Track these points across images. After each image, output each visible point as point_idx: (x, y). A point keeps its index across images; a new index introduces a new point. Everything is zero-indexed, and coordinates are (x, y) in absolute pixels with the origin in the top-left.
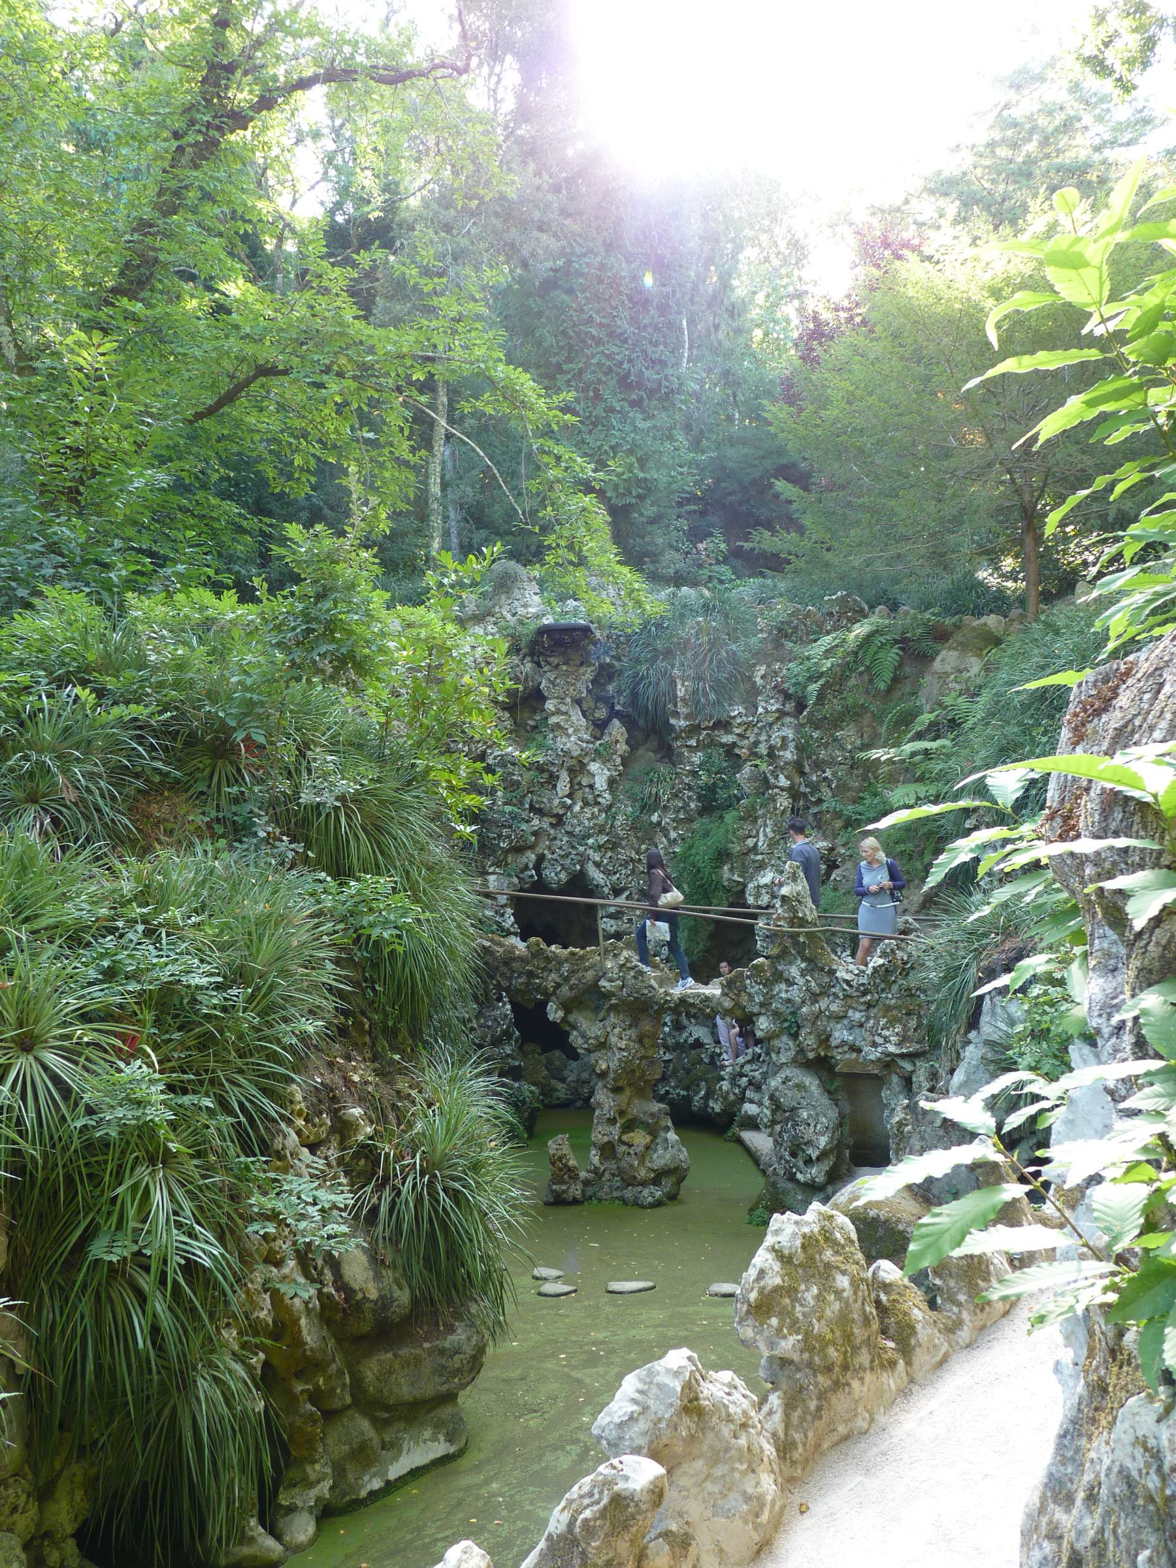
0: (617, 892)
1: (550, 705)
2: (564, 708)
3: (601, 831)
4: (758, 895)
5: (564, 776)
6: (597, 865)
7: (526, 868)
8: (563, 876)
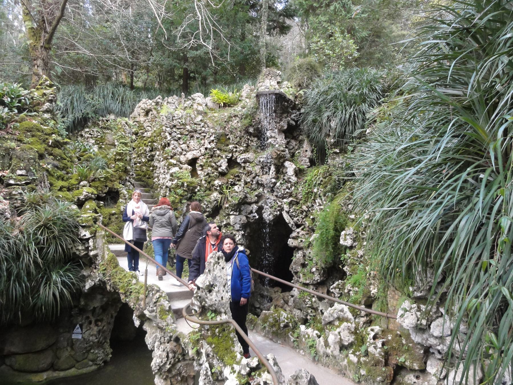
0: (298, 226)
1: (268, 134)
2: (273, 135)
3: (291, 195)
4: (345, 240)
5: (273, 168)
6: (288, 212)
7: (251, 212)
8: (271, 217)
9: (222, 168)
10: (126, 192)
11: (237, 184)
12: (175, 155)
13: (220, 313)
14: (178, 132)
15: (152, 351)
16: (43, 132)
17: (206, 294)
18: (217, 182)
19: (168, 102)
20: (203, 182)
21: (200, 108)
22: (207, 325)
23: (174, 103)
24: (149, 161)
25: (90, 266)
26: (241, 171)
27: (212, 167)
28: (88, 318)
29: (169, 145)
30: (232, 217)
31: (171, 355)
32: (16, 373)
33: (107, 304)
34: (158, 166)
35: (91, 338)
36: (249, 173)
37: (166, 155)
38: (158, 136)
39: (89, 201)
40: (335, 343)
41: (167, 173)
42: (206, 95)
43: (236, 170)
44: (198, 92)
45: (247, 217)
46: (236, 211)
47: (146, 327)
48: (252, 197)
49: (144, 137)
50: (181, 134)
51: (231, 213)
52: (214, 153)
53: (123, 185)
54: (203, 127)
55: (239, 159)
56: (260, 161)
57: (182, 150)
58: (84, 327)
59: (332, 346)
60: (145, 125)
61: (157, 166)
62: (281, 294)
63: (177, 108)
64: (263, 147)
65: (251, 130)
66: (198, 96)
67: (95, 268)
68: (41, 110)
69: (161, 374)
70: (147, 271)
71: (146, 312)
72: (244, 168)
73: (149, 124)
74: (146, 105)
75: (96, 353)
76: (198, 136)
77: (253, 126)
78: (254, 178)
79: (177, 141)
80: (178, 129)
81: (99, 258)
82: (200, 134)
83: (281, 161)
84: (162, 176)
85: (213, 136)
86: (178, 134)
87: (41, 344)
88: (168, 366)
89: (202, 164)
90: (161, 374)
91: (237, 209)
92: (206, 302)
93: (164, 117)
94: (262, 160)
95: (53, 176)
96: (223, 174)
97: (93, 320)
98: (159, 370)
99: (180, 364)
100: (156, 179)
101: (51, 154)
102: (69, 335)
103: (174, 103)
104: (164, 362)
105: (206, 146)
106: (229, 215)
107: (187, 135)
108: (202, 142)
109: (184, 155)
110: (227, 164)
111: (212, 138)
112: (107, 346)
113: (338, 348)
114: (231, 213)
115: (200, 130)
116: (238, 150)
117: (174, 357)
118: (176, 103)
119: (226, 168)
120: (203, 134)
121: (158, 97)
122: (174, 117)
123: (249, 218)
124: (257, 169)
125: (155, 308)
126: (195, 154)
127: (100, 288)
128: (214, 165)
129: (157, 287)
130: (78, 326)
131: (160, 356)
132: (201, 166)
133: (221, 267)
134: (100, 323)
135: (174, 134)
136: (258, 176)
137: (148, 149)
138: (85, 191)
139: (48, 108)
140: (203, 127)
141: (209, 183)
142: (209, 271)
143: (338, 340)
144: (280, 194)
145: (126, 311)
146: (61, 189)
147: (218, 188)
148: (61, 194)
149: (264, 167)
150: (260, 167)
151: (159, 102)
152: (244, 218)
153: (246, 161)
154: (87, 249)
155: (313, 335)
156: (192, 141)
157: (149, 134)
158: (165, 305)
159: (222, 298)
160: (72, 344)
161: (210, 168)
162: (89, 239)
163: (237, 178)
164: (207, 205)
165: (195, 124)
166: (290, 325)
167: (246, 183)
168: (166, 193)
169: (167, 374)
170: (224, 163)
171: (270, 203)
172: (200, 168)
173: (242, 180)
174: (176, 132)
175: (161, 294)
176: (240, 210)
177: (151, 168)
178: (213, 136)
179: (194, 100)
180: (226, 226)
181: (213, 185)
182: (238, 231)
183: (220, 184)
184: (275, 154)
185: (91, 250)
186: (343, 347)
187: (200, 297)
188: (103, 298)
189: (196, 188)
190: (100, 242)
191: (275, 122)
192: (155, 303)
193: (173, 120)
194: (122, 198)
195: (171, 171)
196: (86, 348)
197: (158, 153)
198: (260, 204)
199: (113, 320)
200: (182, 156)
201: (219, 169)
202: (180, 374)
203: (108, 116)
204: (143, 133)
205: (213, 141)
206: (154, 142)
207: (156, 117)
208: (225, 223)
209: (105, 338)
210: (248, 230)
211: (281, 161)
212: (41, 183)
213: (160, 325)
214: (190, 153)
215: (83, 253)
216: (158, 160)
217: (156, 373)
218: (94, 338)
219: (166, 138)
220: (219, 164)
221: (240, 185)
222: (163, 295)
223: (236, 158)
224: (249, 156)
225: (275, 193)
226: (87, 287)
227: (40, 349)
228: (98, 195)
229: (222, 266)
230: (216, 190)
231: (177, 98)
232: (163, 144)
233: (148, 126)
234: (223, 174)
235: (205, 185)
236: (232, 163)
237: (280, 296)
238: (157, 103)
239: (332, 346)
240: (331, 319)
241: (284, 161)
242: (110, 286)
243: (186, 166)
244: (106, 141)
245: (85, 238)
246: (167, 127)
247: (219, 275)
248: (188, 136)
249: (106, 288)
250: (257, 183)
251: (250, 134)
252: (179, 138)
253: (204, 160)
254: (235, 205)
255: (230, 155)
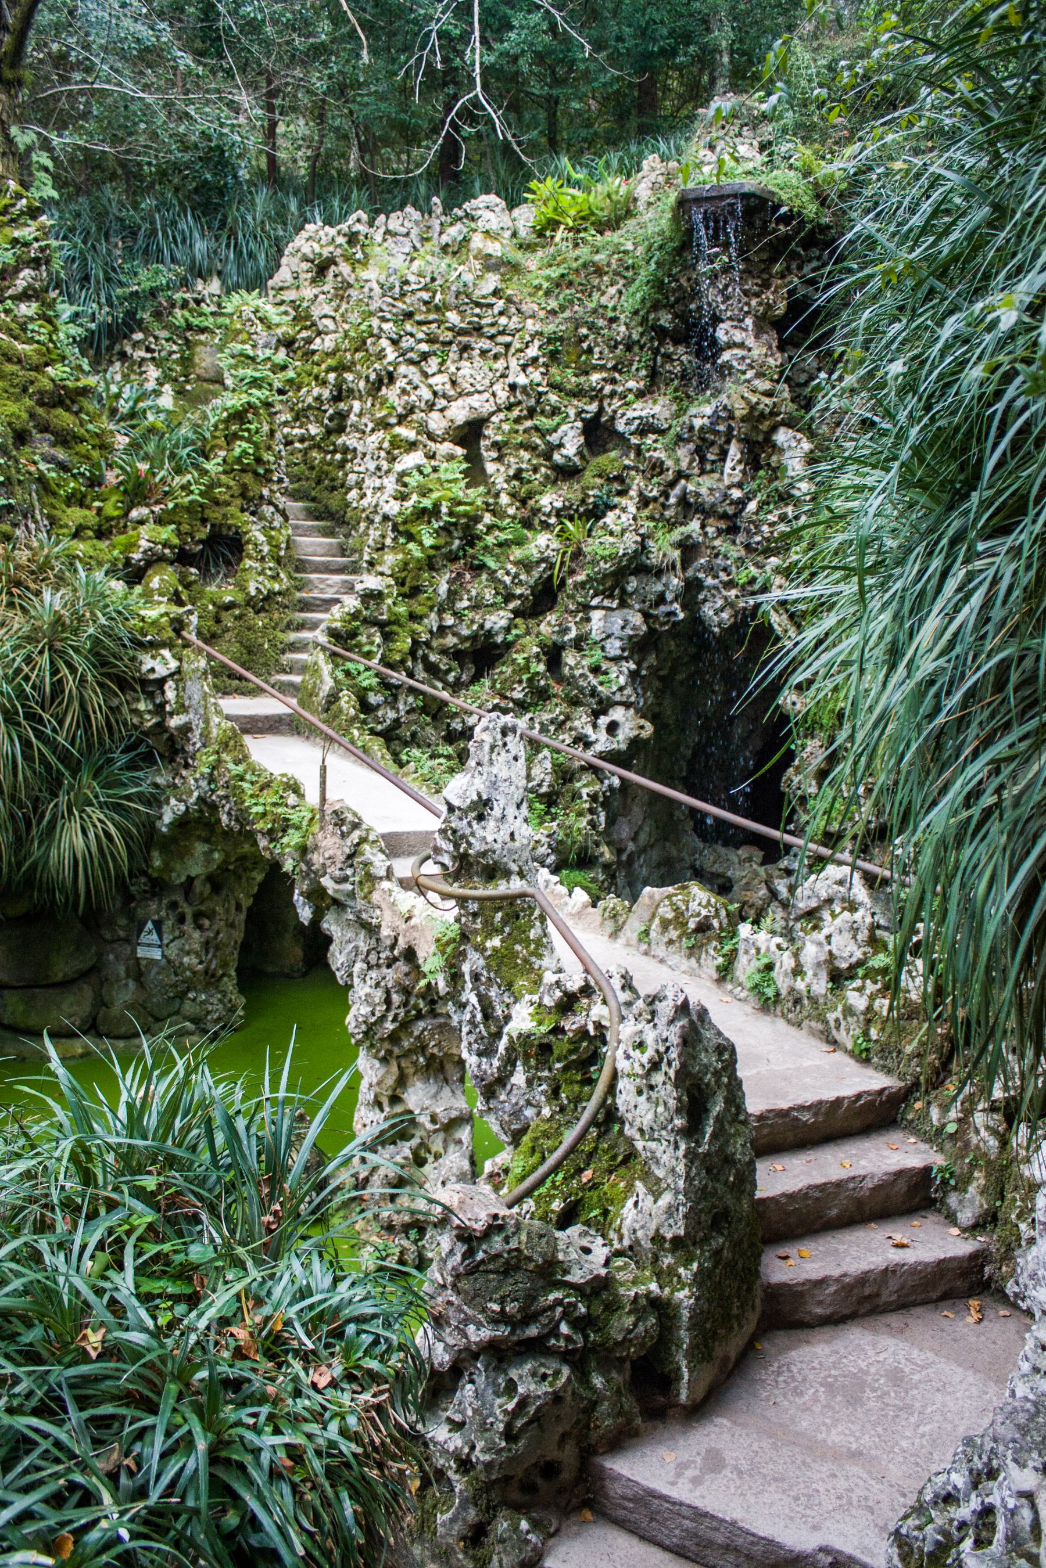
2: (738, 336)
5: (734, 451)
7: (661, 599)
9: (564, 451)
10: (262, 538)
11: (615, 507)
12: (411, 410)
13: (507, 874)
14: (421, 336)
15: (349, 987)
16: (20, 361)
17: (469, 824)
18: (549, 500)
19: (388, 232)
20: (504, 499)
21: (495, 249)
22: (475, 899)
23: (407, 235)
24: (329, 432)
25: (172, 760)
26: (627, 462)
27: (532, 448)
28: (174, 905)
29: (391, 378)
30: (596, 615)
31: (396, 998)
32: (7, 1035)
33: (223, 868)
34: (360, 449)
35: (186, 960)
36: (657, 468)
37: (384, 412)
38: (357, 350)
39: (156, 567)
40: (819, 964)
41: (389, 471)
42: (512, 203)
43: (612, 459)
44: (487, 193)
45: (646, 616)
46: (611, 596)
47: (331, 925)
48: (664, 548)
49: (314, 352)
50: (431, 340)
51: (594, 602)
52: (538, 402)
53: (253, 514)
54: (501, 313)
55: (623, 421)
56: (691, 428)
57: (435, 393)
58: (165, 928)
59: (810, 973)
60: (316, 312)
61: (355, 450)
62: (761, 871)
63: (415, 248)
64: (691, 384)
65: (665, 319)
66: (488, 209)
67: (187, 766)
68: (10, 292)
69: (372, 1046)
70: (324, 769)
71: (326, 882)
72: (639, 452)
73: (328, 310)
74: (316, 246)
75: (202, 1002)
76: (485, 344)
77: (672, 306)
78: (672, 484)
79: (416, 363)
80: (420, 323)
81: (195, 737)
82: (492, 338)
83: (765, 426)
84: (370, 483)
85: (537, 343)
86: (420, 341)
87: (62, 968)
88: (390, 1026)
89: (499, 438)
90: (372, 1046)
91: (612, 589)
92: (469, 844)
93: (375, 286)
94: (698, 423)
95: (55, 494)
96: (567, 473)
97: (188, 911)
98: (366, 1033)
99: (421, 1024)
100: (353, 494)
101: (44, 429)
102: (129, 949)
103: (407, 235)
104: (378, 1014)
105: (510, 380)
106: (586, 608)
107: (450, 343)
108: (500, 365)
109: (442, 410)
110: (582, 439)
111: (532, 352)
112: (230, 984)
113: (824, 976)
114: (594, 603)
115: (492, 325)
116: (620, 389)
117: (405, 1004)
118: (414, 232)
119: (580, 453)
120: (501, 339)
121: (354, 217)
122: (407, 282)
123: (656, 617)
124: (683, 453)
125: (349, 872)
126: (476, 405)
127: (200, 822)
128: (539, 441)
129: (355, 814)
130: (150, 925)
131: (368, 999)
132: (496, 445)
133: (510, 756)
134: (206, 923)
135: (407, 343)
136: (687, 477)
137: (326, 394)
138: (149, 536)
139: (30, 286)
140: (501, 313)
141: (524, 502)
142: (478, 764)
143: (823, 957)
144: (758, 538)
145: (276, 883)
146: (76, 535)
147: (553, 520)
148: (81, 548)
149: (707, 447)
150: (691, 446)
151: (357, 233)
152: (637, 619)
153: (646, 428)
154: (160, 709)
155: (768, 949)
156: (465, 364)
157: (328, 343)
158: (377, 863)
159: (512, 834)
160: (138, 971)
161: (525, 455)
162: (162, 681)
163: (617, 486)
164: (516, 576)
165: (478, 305)
166: (715, 923)
167: (644, 502)
168: (383, 537)
169: (387, 1045)
170: (571, 433)
171: (725, 570)
172: (494, 454)
173: (633, 493)
174: (412, 335)
175: (364, 834)
176: (623, 591)
177: (338, 456)
178: (537, 343)
179: (473, 219)
180: (579, 643)
181: (536, 511)
182: (615, 660)
183: (558, 504)
184: (743, 405)
185: (171, 714)
186: (838, 978)
187: (454, 832)
188: (211, 851)
189: (477, 519)
190: (198, 689)
191: (746, 293)
192: (350, 857)
193: (403, 295)
194: (250, 558)
195: (398, 467)
196: (175, 985)
197: (357, 405)
198: (690, 573)
199: (243, 916)
200: (435, 415)
201: (557, 457)
202: (423, 1048)
203: (200, 285)
204: (309, 341)
205: (535, 360)
206: (348, 369)
207: (350, 286)
208: (573, 634)
209: (224, 965)
210: (652, 659)
211: (765, 426)
212: (25, 517)
213: (364, 916)
214: (460, 402)
215: (150, 721)
216: (358, 430)
217: (359, 1043)
218: (195, 961)
219: (381, 356)
220: (554, 438)
221: (624, 510)
222: (371, 838)
223: (613, 419)
224: (657, 409)
225: (740, 538)
226: (168, 818)
227: (60, 976)
228: (181, 549)
229: (513, 753)
230: (546, 526)
231: (416, 215)
232: (373, 376)
233: (325, 316)
234: (567, 473)
235: (511, 511)
236: (598, 433)
237: (756, 874)
238: (352, 238)
239: (810, 973)
240: (813, 903)
241: (774, 429)
242: (229, 814)
243: (446, 447)
244: (198, 371)
245: (152, 677)
246: (384, 320)
247: (504, 774)
248: (454, 347)
249: (219, 821)
250: (683, 500)
251: (661, 333)
252: (425, 356)
253: (506, 427)
254: (605, 576)
255: (594, 407)
